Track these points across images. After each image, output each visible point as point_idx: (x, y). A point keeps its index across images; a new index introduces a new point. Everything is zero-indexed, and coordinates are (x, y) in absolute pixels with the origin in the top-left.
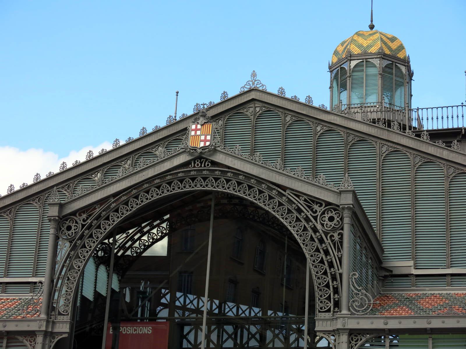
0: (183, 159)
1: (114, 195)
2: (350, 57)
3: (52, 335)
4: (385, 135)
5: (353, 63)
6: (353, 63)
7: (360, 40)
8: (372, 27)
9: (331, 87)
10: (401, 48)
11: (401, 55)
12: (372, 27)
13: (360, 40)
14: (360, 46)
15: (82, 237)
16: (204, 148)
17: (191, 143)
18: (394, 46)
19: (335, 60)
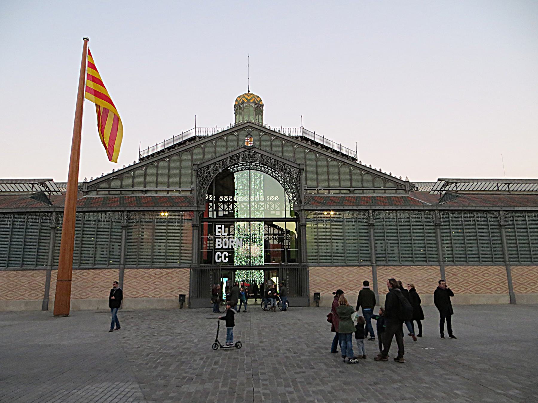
0: (243, 150)
1: (218, 162)
2: (243, 102)
3: (199, 211)
4: (296, 142)
5: (245, 105)
6: (245, 105)
7: (247, 97)
8: (249, 91)
9: (235, 114)
10: (261, 100)
11: (261, 103)
12: (249, 91)
13: (247, 97)
14: (247, 99)
15: (207, 177)
16: (251, 146)
17: (246, 144)
18: (259, 100)
19: (237, 103)
